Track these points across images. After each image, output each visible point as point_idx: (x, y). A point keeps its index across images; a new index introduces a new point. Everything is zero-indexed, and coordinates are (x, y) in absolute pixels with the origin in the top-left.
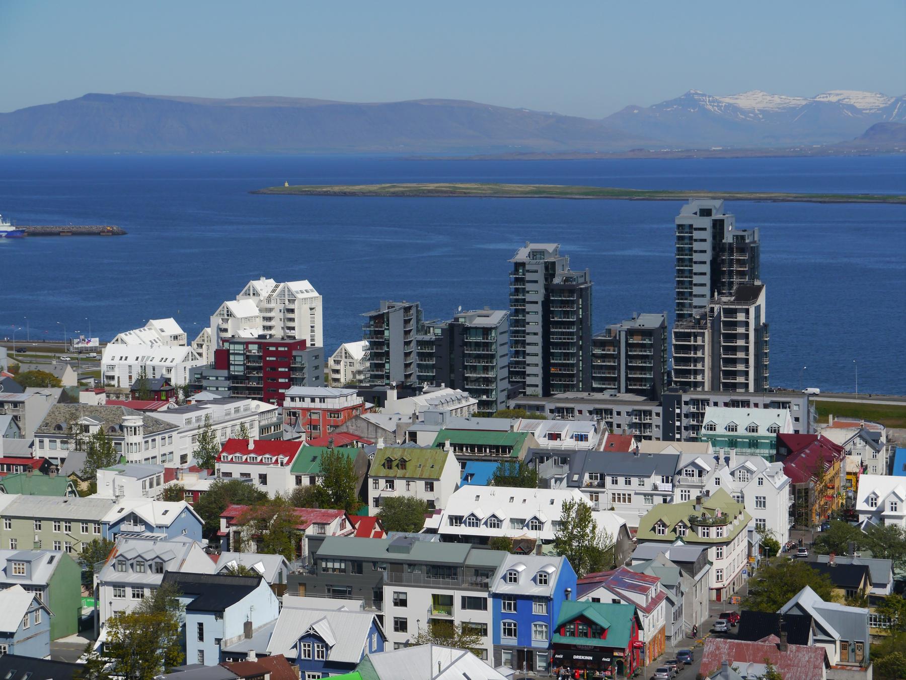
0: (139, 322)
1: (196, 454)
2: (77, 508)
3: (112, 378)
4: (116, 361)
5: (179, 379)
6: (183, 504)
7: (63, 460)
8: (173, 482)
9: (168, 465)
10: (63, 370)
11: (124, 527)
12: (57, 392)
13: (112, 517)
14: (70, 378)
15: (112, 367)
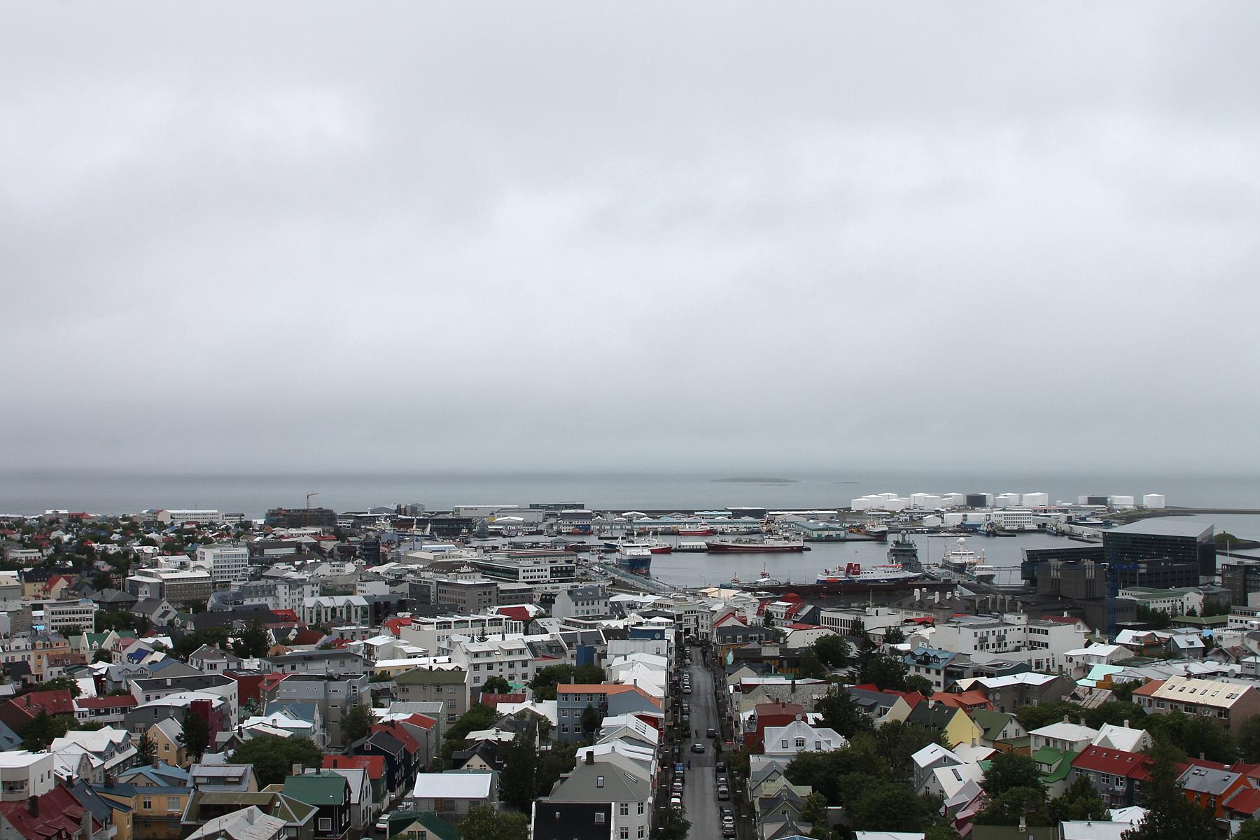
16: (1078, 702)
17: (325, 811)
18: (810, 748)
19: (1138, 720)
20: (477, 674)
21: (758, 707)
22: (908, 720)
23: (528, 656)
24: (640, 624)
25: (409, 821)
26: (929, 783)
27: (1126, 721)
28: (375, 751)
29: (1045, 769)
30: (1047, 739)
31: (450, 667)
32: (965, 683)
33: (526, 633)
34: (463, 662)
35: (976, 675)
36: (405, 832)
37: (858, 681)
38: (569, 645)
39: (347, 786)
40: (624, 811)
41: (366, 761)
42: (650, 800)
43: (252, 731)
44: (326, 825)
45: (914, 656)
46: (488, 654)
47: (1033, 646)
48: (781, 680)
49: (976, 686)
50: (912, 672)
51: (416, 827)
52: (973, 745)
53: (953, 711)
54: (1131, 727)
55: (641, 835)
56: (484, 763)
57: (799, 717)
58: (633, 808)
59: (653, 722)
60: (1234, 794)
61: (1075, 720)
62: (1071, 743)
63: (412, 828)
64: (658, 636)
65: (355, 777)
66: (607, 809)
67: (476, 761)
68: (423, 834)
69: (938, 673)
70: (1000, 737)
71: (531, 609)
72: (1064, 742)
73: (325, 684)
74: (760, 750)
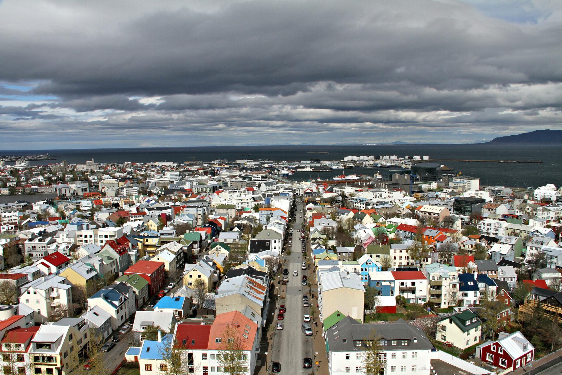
0: (545, 185)
1: (555, 217)
2: (524, 227)
3: (536, 197)
4: (538, 194)
5: (554, 199)
6: (550, 229)
7: (522, 216)
8: (548, 224)
9: (548, 219)
10: (524, 195)
11: (534, 233)
12: (522, 200)
13: (532, 230)
14: (526, 197)
15: (536, 195)
16: (399, 212)
17: (195, 242)
18: (326, 225)
19: (416, 217)
20: (238, 206)
21: (312, 214)
22: (353, 217)
23: (253, 200)
24: (283, 192)
25: (217, 245)
26: (357, 234)
27: (412, 217)
28: (209, 227)
29: (389, 230)
30: (391, 222)
31: (230, 204)
32: (370, 207)
33: (253, 194)
34: (234, 202)
35: (373, 205)
36: (215, 248)
37: (341, 207)
38: (264, 197)
39: (201, 236)
40: (275, 242)
41: (207, 229)
42: (282, 239)
43: (177, 221)
44: (195, 246)
45: (357, 200)
46: (242, 200)
47: (390, 197)
48: (320, 206)
49: (372, 208)
50: (356, 205)
51: (218, 246)
52: (371, 224)
53: (365, 215)
54: (413, 218)
55: (279, 248)
56: (238, 229)
57: (323, 216)
58: (277, 241)
59: (285, 218)
60: (438, 236)
61: (398, 217)
62: (397, 223)
63: (217, 247)
64: (287, 195)
65: (203, 234)
66: (269, 241)
67: (236, 229)
68: (220, 248)
69: (363, 204)
70: (378, 222)
71: (255, 188)
72: (395, 223)
73: (197, 209)
74: (313, 225)
